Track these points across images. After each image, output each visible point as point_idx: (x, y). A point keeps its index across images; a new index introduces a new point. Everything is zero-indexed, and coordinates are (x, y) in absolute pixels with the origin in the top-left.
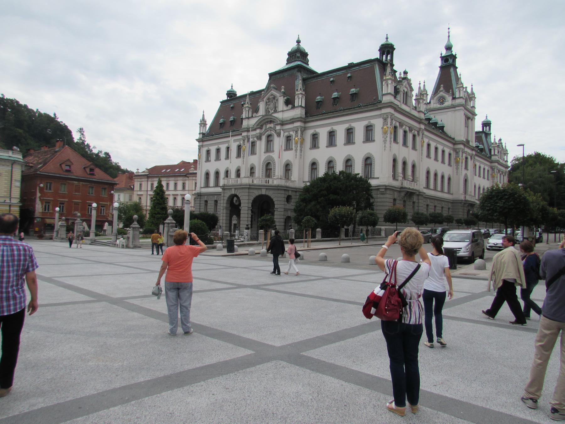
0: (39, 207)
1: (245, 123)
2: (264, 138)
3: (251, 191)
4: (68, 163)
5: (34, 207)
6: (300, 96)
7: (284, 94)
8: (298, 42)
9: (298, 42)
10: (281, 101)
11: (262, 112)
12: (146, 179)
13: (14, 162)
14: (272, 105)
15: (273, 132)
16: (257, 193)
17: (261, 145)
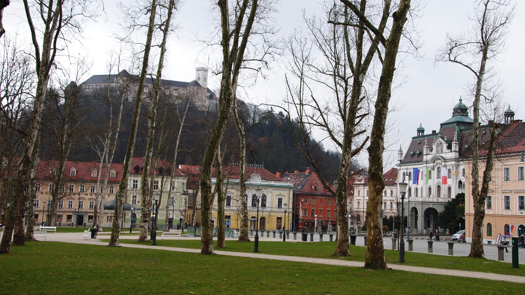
0: (301, 213)
1: (425, 158)
2: (436, 169)
3: (423, 205)
4: (316, 185)
5: (299, 213)
6: (455, 145)
7: (446, 142)
8: (461, 100)
9: (461, 100)
10: (445, 145)
11: (434, 151)
12: (363, 187)
13: (290, 188)
14: (440, 148)
15: (441, 166)
16: (427, 207)
17: (434, 173)
